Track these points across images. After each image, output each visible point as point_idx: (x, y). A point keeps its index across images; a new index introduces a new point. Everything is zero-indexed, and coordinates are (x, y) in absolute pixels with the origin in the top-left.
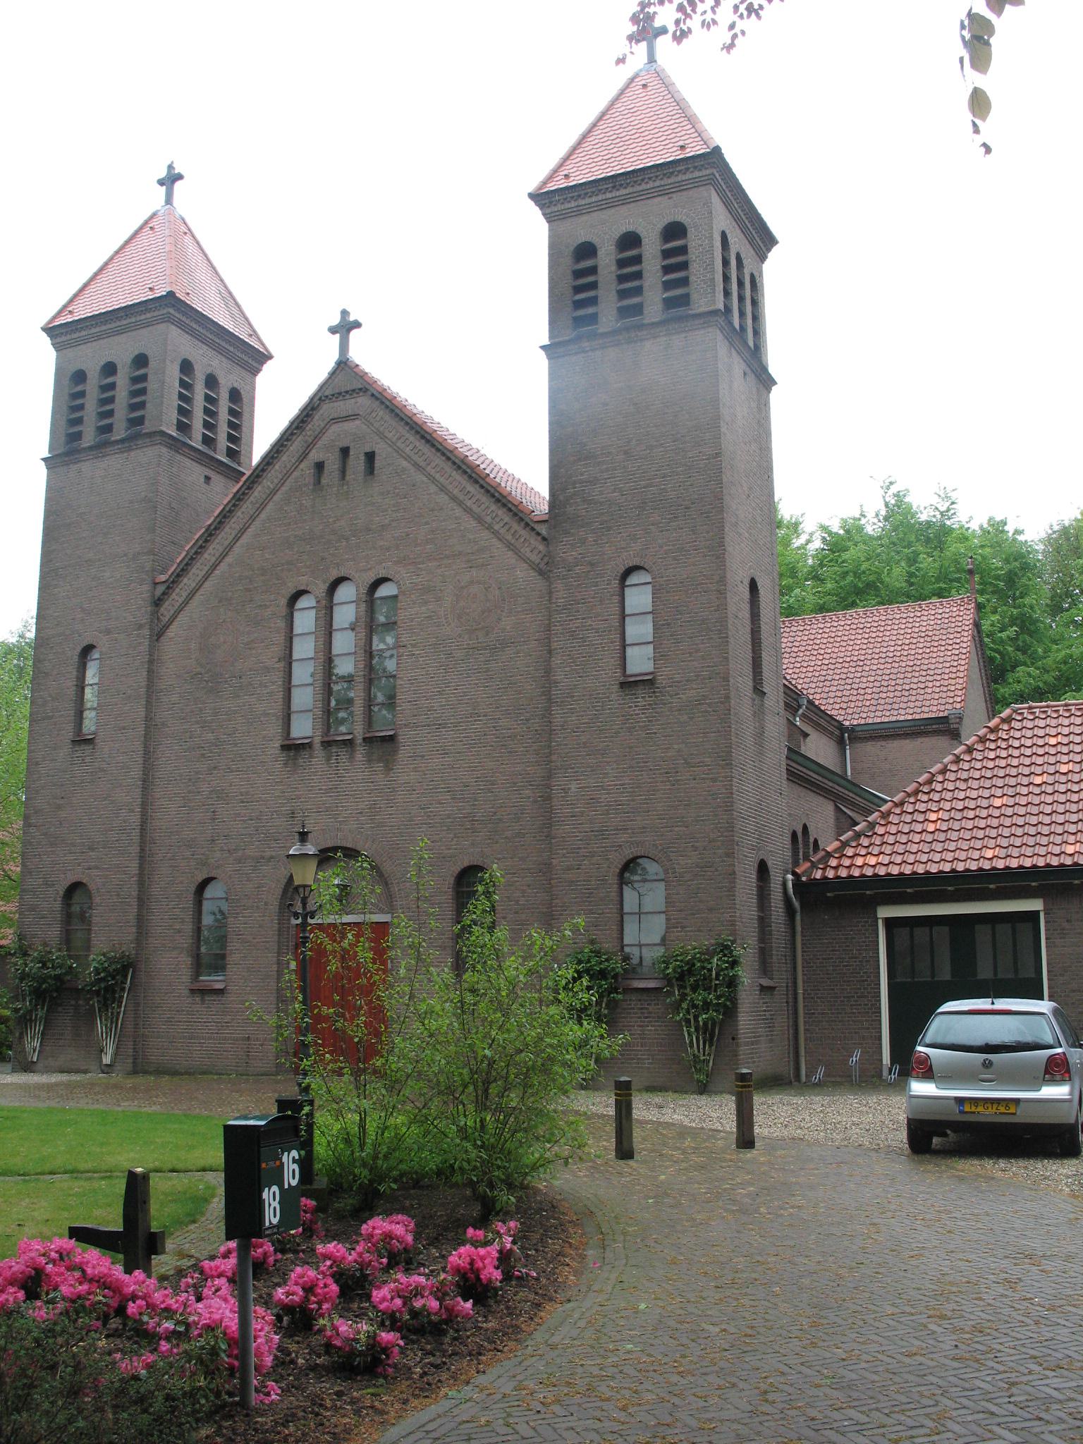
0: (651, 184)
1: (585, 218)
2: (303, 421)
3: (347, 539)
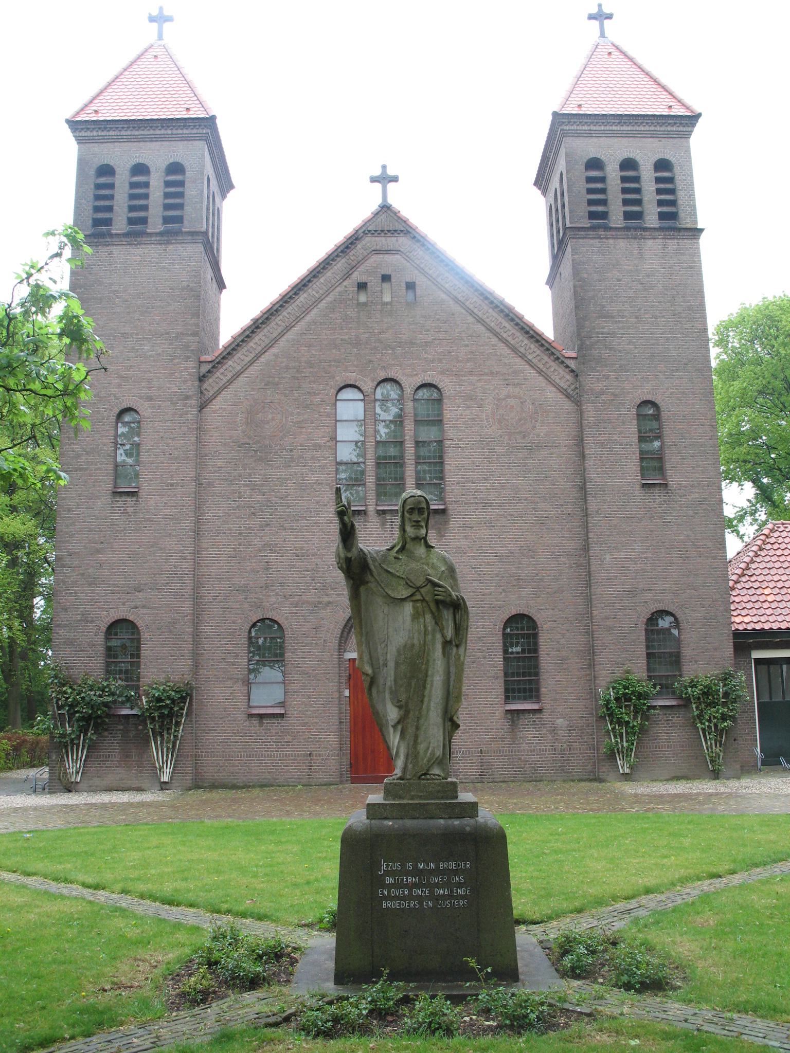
0: (647, 128)
1: (595, 140)
2: (347, 247)
3: (393, 349)
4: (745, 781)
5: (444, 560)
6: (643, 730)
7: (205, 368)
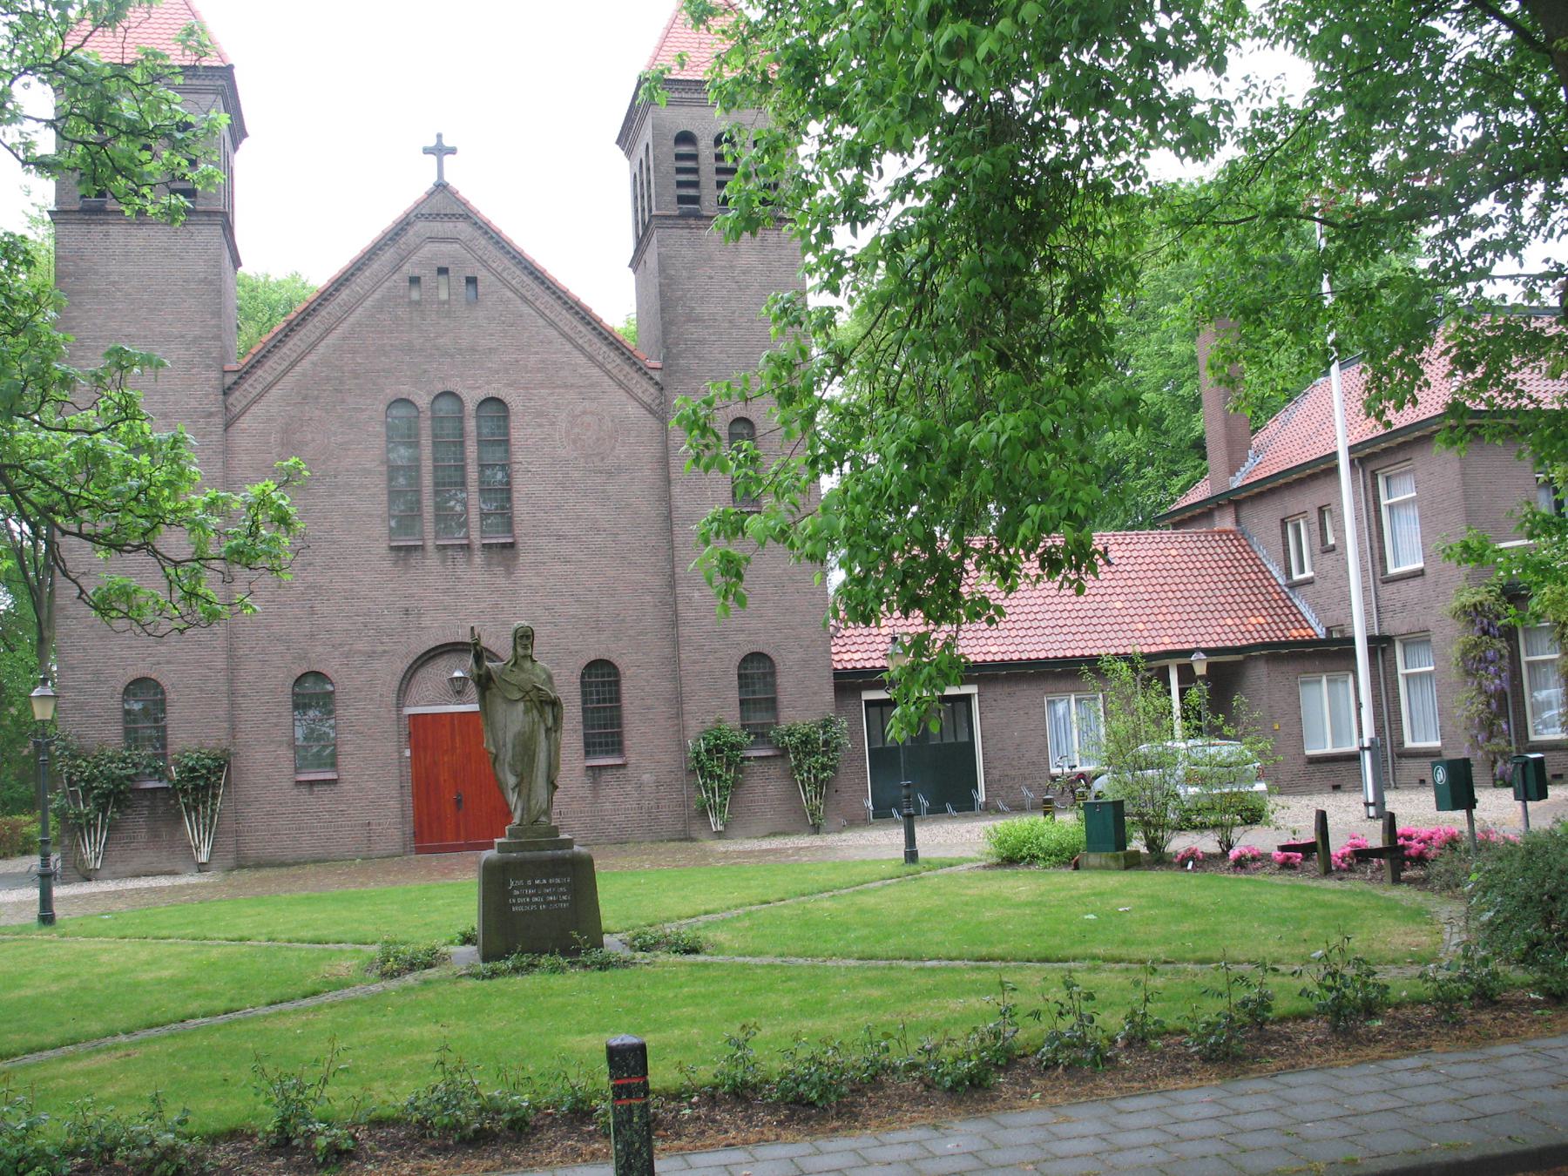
4: (844, 836)
5: (544, 670)
6: (736, 783)
7: (230, 379)
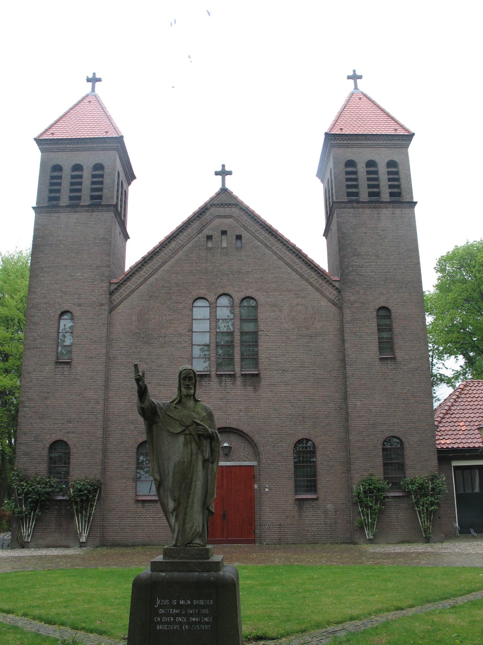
0: (382, 142)
2: (201, 214)
3: (228, 275)
4: (446, 545)
5: (206, 409)
6: (381, 511)
7: (113, 287)
